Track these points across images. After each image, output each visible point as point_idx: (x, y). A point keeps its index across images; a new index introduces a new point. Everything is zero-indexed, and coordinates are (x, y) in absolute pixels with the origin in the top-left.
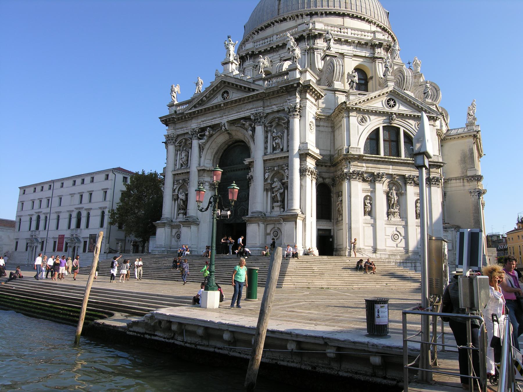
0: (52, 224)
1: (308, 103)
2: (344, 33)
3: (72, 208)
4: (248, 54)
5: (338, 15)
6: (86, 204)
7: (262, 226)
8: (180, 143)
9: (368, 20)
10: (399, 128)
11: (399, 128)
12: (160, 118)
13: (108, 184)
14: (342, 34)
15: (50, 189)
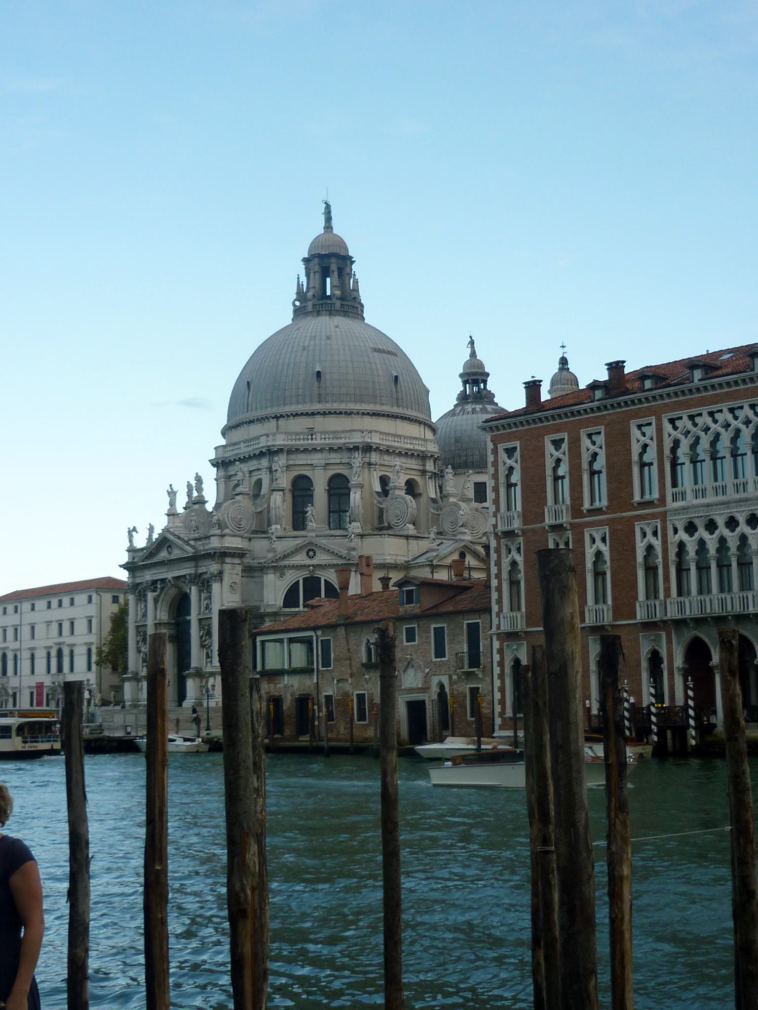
0: (25, 665)
1: (227, 567)
2: (312, 439)
3: (50, 643)
4: (218, 463)
5: (307, 414)
6: (67, 639)
7: (198, 680)
8: (140, 592)
9: (346, 413)
10: (320, 578)
11: (320, 578)
12: (120, 566)
13: (92, 610)
14: (310, 441)
15: (16, 611)
